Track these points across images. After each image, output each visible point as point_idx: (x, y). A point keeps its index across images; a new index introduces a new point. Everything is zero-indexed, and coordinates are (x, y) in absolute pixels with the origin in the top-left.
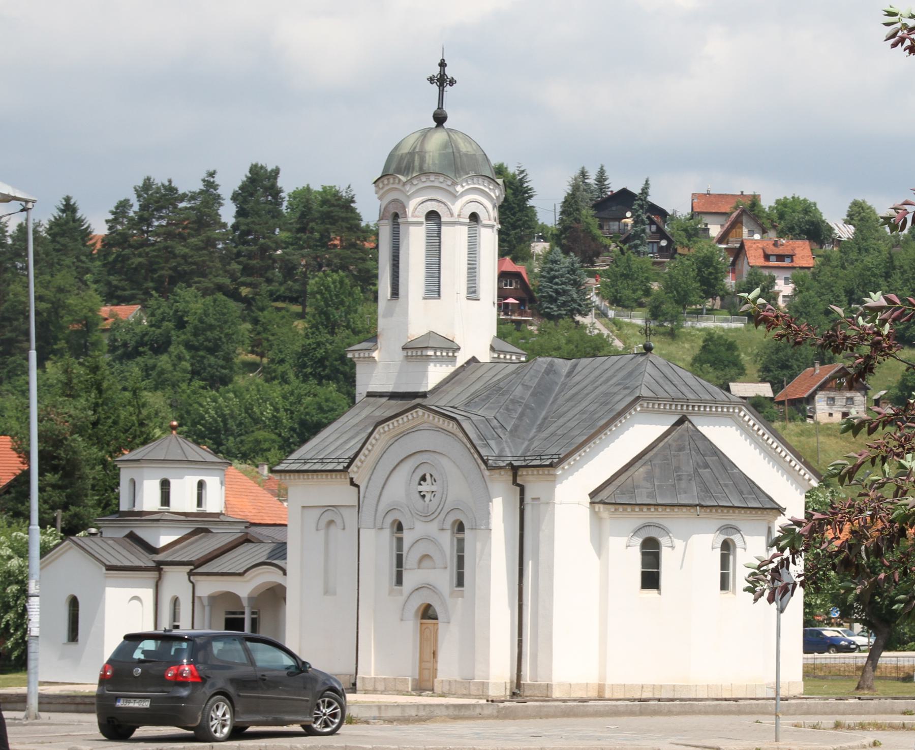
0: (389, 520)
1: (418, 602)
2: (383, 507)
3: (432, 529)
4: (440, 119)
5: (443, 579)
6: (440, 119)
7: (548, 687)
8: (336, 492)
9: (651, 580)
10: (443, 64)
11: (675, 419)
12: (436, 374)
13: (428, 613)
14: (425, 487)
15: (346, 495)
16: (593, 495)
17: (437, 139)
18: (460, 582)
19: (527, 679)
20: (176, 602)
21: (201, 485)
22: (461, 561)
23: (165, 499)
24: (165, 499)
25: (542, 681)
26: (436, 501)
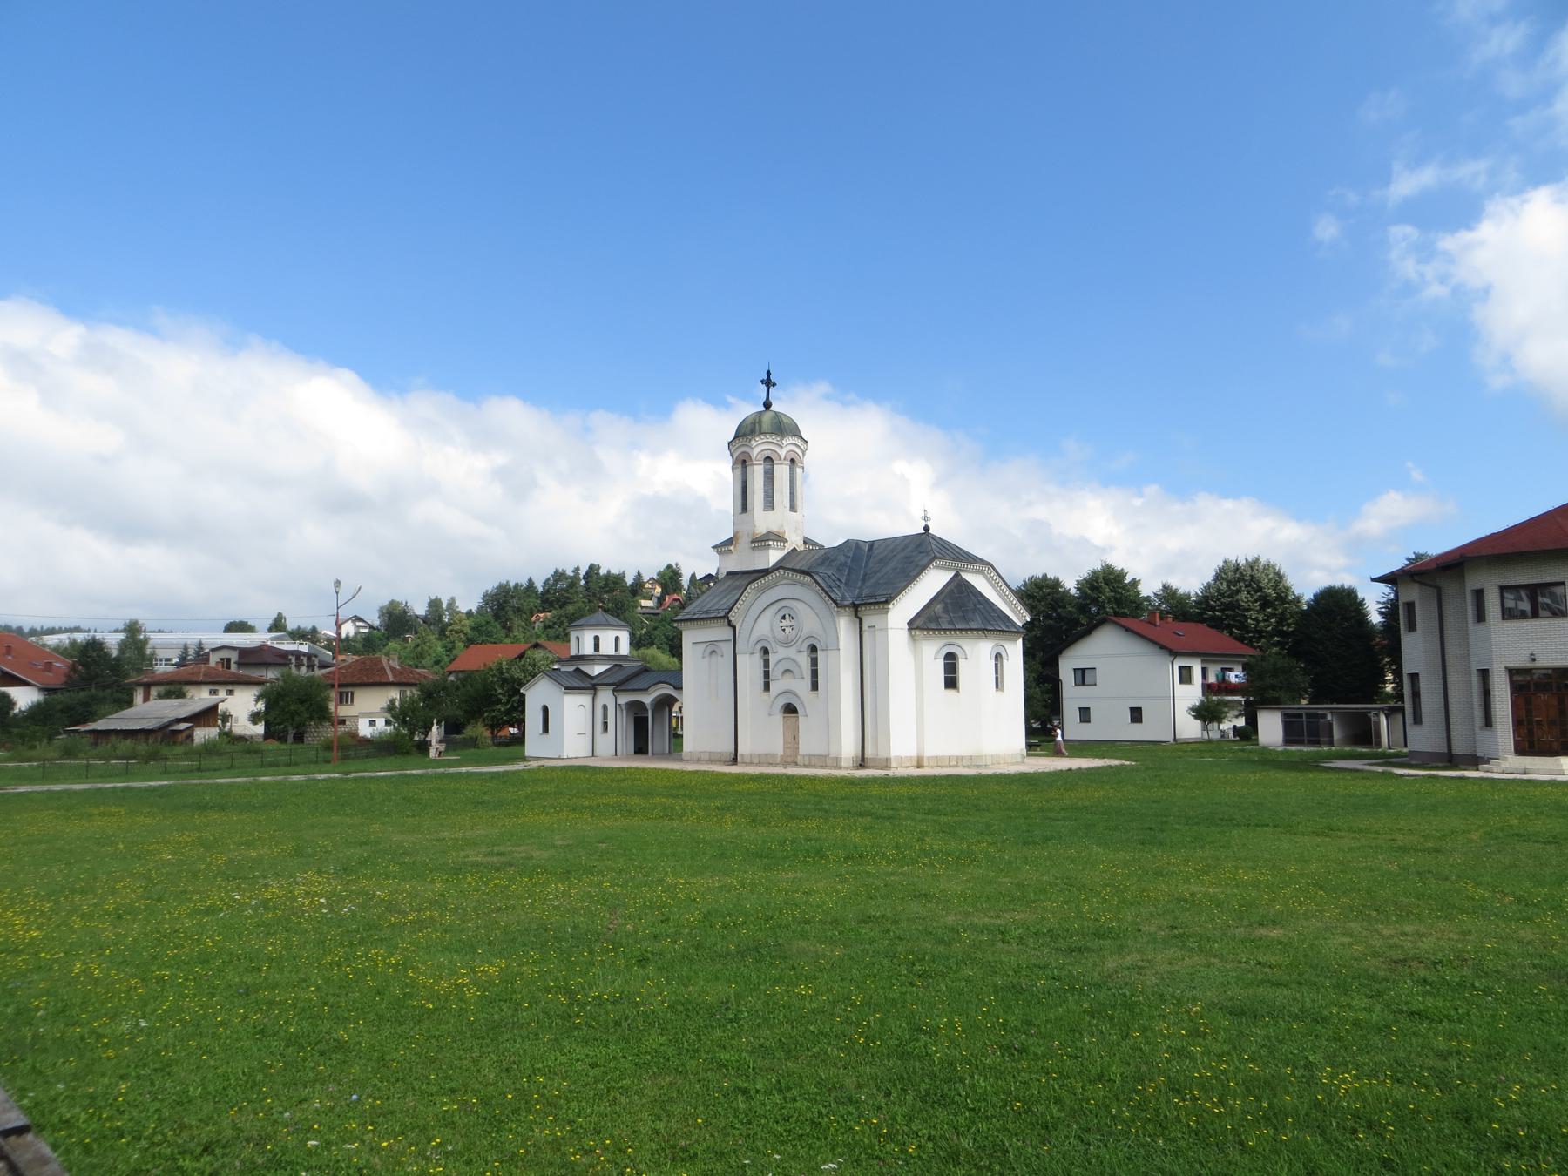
0: (759, 647)
1: (782, 701)
2: (753, 638)
3: (791, 653)
4: (767, 405)
5: (802, 686)
6: (767, 405)
7: (888, 760)
8: (720, 633)
9: (951, 683)
10: (769, 373)
11: (950, 575)
12: (774, 556)
13: (790, 709)
14: (784, 623)
15: (726, 633)
16: (910, 623)
17: (767, 417)
18: (815, 686)
19: (869, 753)
20: (605, 707)
21: (617, 638)
22: (815, 674)
23: (597, 647)
24: (597, 647)
25: (882, 755)
26: (793, 633)
